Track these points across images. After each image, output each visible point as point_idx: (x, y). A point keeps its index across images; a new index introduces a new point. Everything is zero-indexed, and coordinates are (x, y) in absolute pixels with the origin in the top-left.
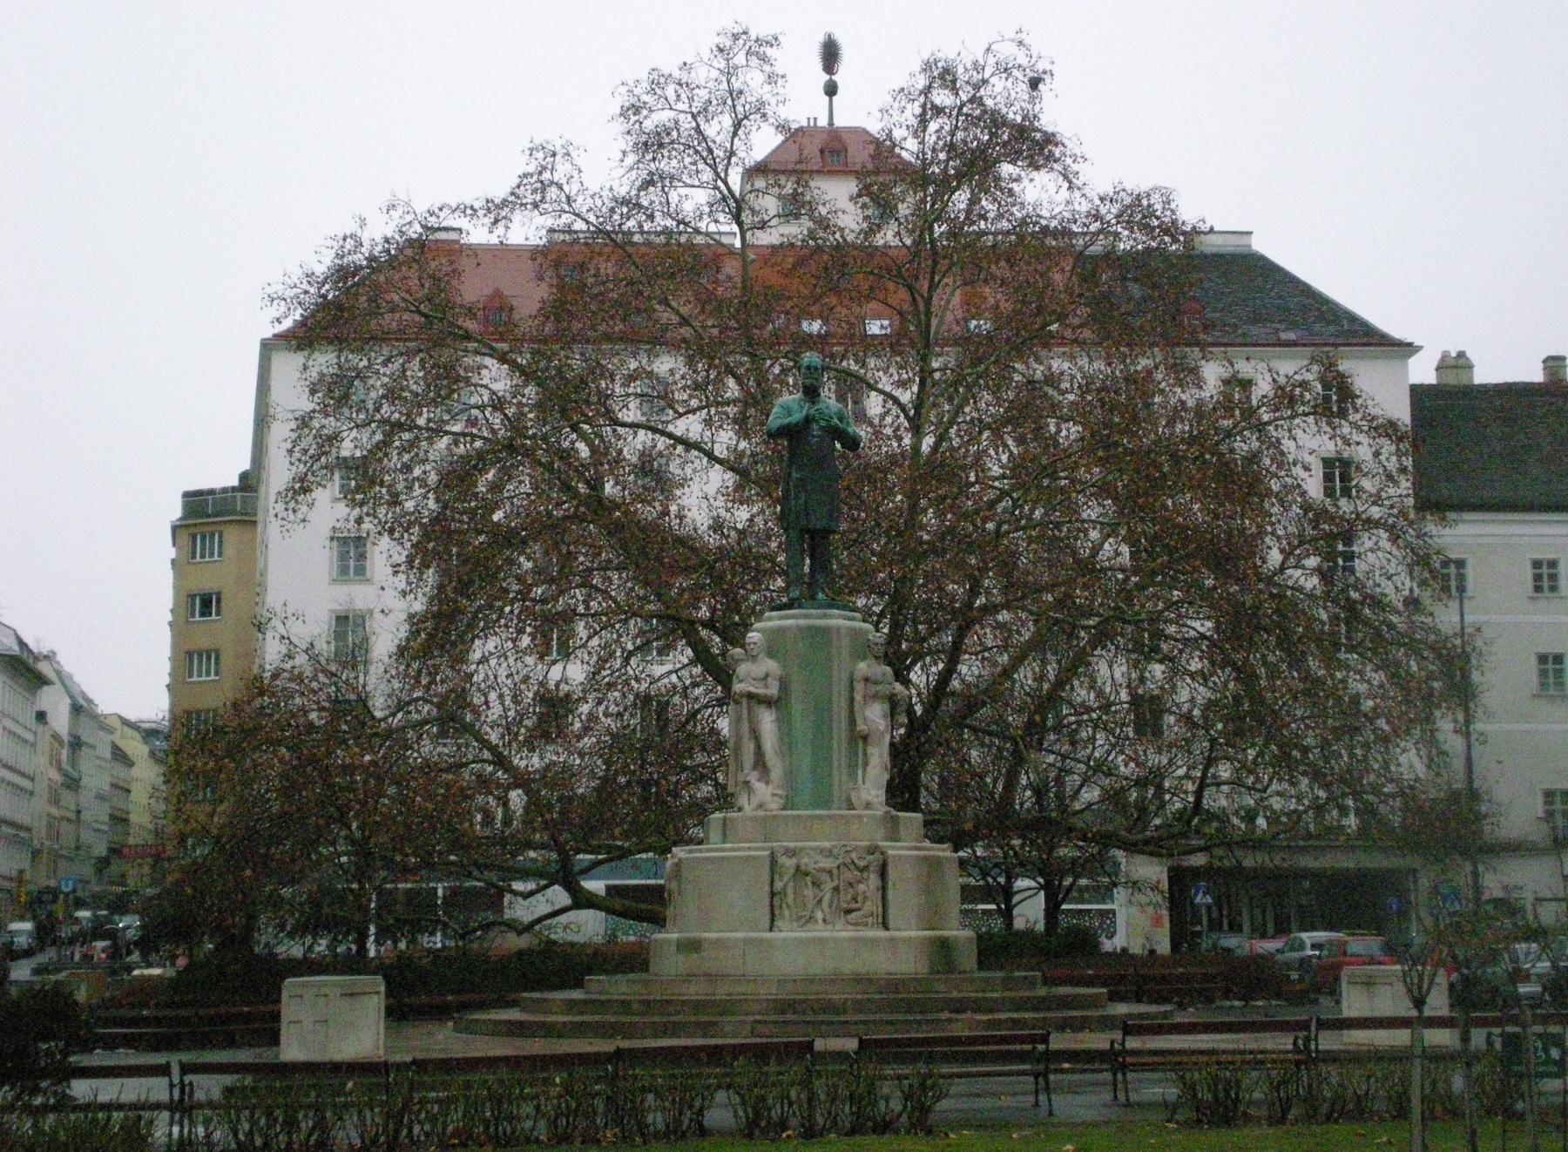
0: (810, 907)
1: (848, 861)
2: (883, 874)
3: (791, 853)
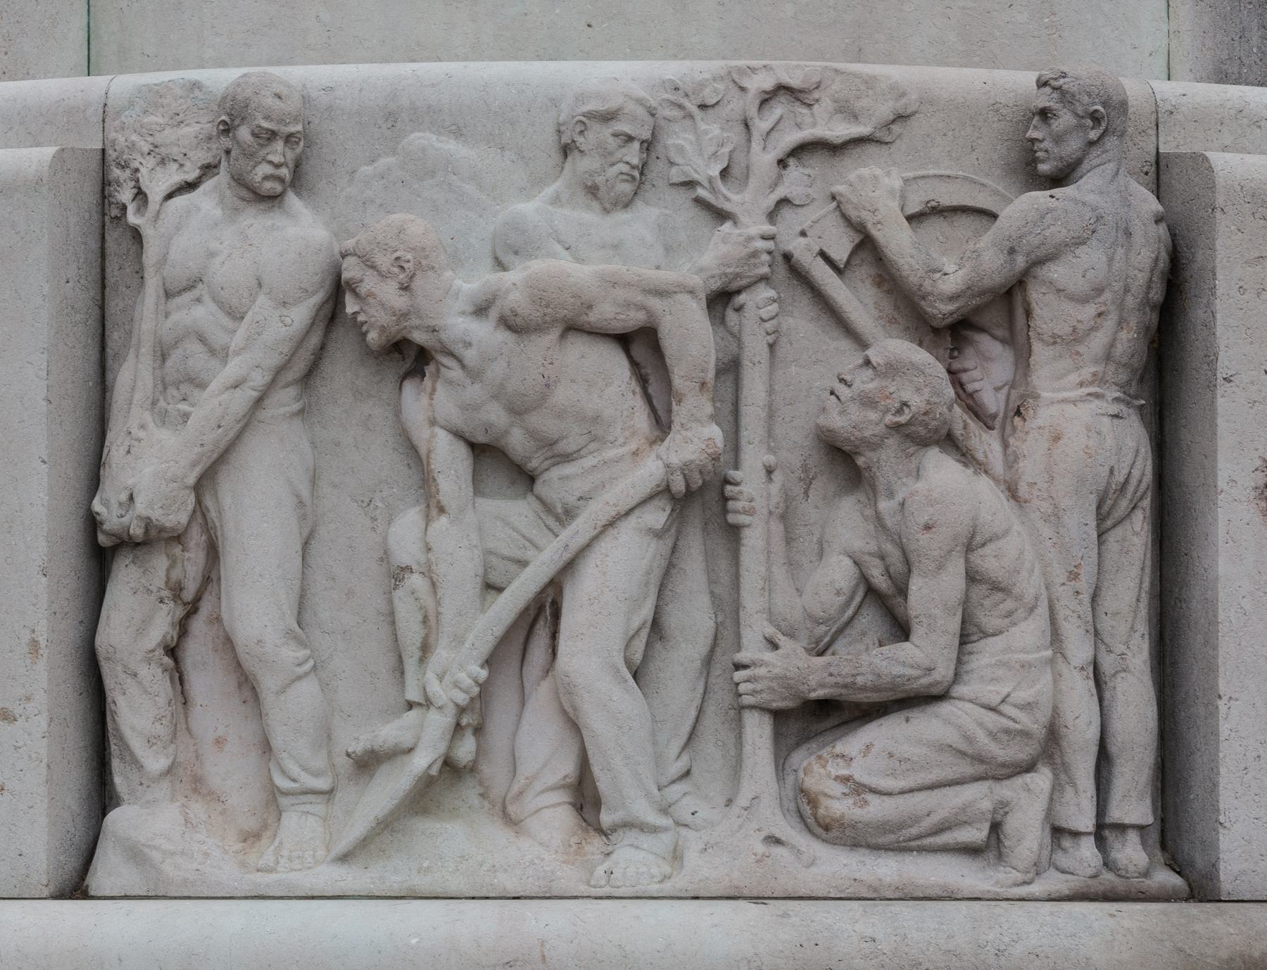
0: (456, 668)
1: (817, 235)
2: (1164, 365)
3: (265, 156)
